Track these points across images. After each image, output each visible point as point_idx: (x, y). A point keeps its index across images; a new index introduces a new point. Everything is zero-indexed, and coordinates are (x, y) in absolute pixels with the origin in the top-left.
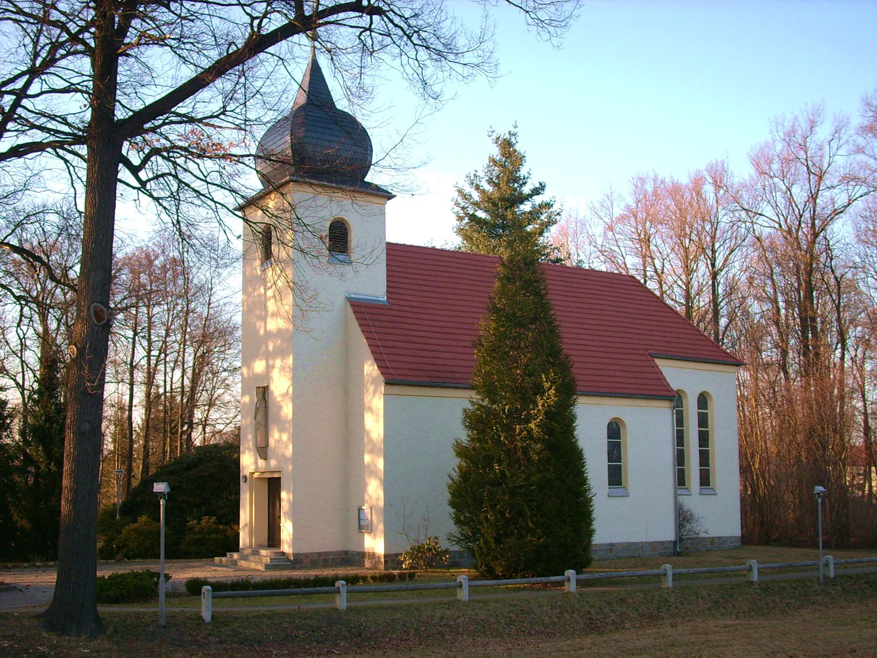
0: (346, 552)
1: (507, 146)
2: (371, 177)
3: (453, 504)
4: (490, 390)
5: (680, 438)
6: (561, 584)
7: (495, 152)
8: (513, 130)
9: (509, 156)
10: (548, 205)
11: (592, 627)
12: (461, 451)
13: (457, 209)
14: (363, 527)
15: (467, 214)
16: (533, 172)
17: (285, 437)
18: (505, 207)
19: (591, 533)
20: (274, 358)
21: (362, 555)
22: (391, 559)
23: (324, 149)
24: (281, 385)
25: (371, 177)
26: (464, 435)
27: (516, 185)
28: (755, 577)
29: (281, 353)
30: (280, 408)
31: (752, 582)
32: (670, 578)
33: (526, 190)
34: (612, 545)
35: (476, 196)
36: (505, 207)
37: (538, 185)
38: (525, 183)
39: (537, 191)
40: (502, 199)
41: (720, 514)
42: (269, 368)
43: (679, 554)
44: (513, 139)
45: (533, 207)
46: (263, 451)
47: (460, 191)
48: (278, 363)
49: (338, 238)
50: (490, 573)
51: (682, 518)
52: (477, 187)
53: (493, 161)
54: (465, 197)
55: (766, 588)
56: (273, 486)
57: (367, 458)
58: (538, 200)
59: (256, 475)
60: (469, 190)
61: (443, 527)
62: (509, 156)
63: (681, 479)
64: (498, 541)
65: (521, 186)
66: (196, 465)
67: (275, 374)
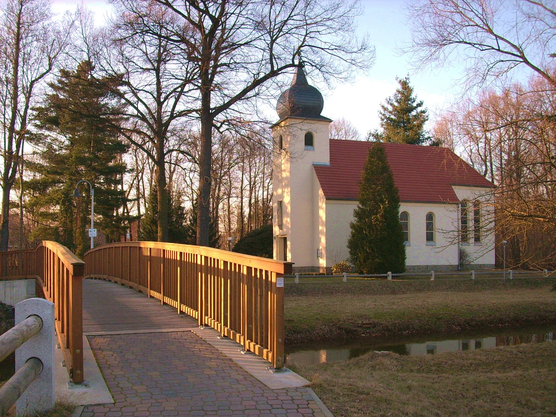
0: (313, 267)
1: (404, 84)
2: (323, 114)
3: (348, 247)
4: (362, 203)
5: (464, 221)
6: (386, 277)
7: (399, 87)
8: (407, 77)
9: (406, 89)
10: (424, 112)
11: (394, 292)
12: (353, 226)
13: (380, 115)
14: (318, 256)
15: (386, 117)
16: (418, 95)
17: (289, 220)
18: (404, 114)
19: (404, 258)
20: (285, 188)
21: (319, 268)
22: (328, 269)
23: (304, 103)
24: (287, 199)
25: (323, 114)
26: (354, 220)
27: (410, 102)
28: (473, 278)
29: (286, 186)
30: (287, 208)
31: (472, 280)
32: (433, 276)
33: (415, 105)
34: (428, 266)
35: (390, 108)
36: (404, 114)
37: (419, 102)
38: (414, 101)
39: (420, 105)
40: (401, 110)
41: (483, 254)
42: (283, 192)
43: (460, 270)
44: (408, 81)
45: (417, 112)
46: (281, 226)
47: (383, 107)
48: (286, 190)
49: (309, 140)
50: (362, 273)
51: (462, 255)
52: (391, 104)
53: (399, 92)
54: (385, 109)
55: (476, 282)
56: (285, 239)
57: (320, 228)
58: (419, 109)
59: (280, 236)
60: (386, 105)
61: (345, 255)
62: (406, 89)
63: (464, 239)
64: (364, 261)
65: (412, 102)
66: (261, 233)
67: (285, 194)
